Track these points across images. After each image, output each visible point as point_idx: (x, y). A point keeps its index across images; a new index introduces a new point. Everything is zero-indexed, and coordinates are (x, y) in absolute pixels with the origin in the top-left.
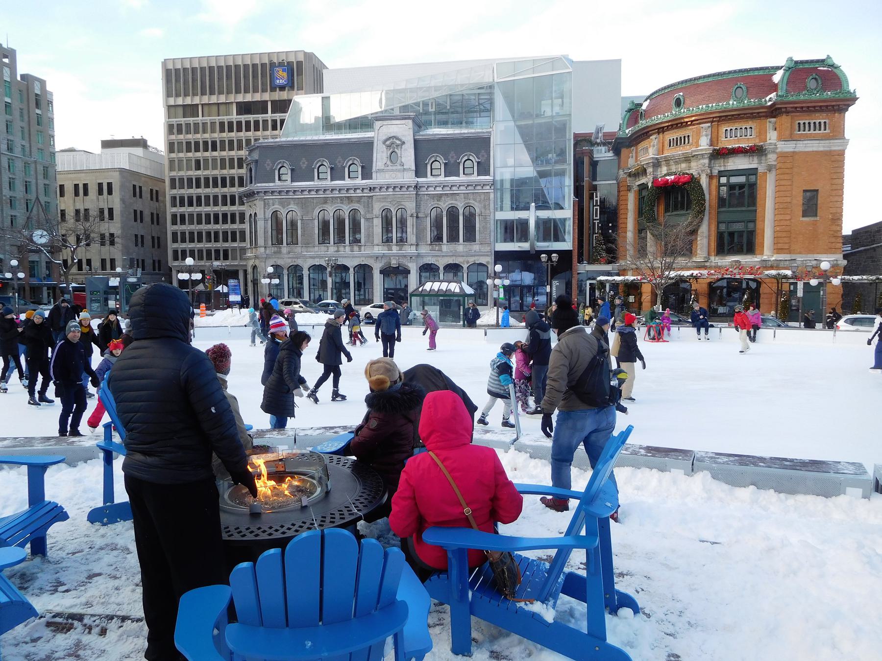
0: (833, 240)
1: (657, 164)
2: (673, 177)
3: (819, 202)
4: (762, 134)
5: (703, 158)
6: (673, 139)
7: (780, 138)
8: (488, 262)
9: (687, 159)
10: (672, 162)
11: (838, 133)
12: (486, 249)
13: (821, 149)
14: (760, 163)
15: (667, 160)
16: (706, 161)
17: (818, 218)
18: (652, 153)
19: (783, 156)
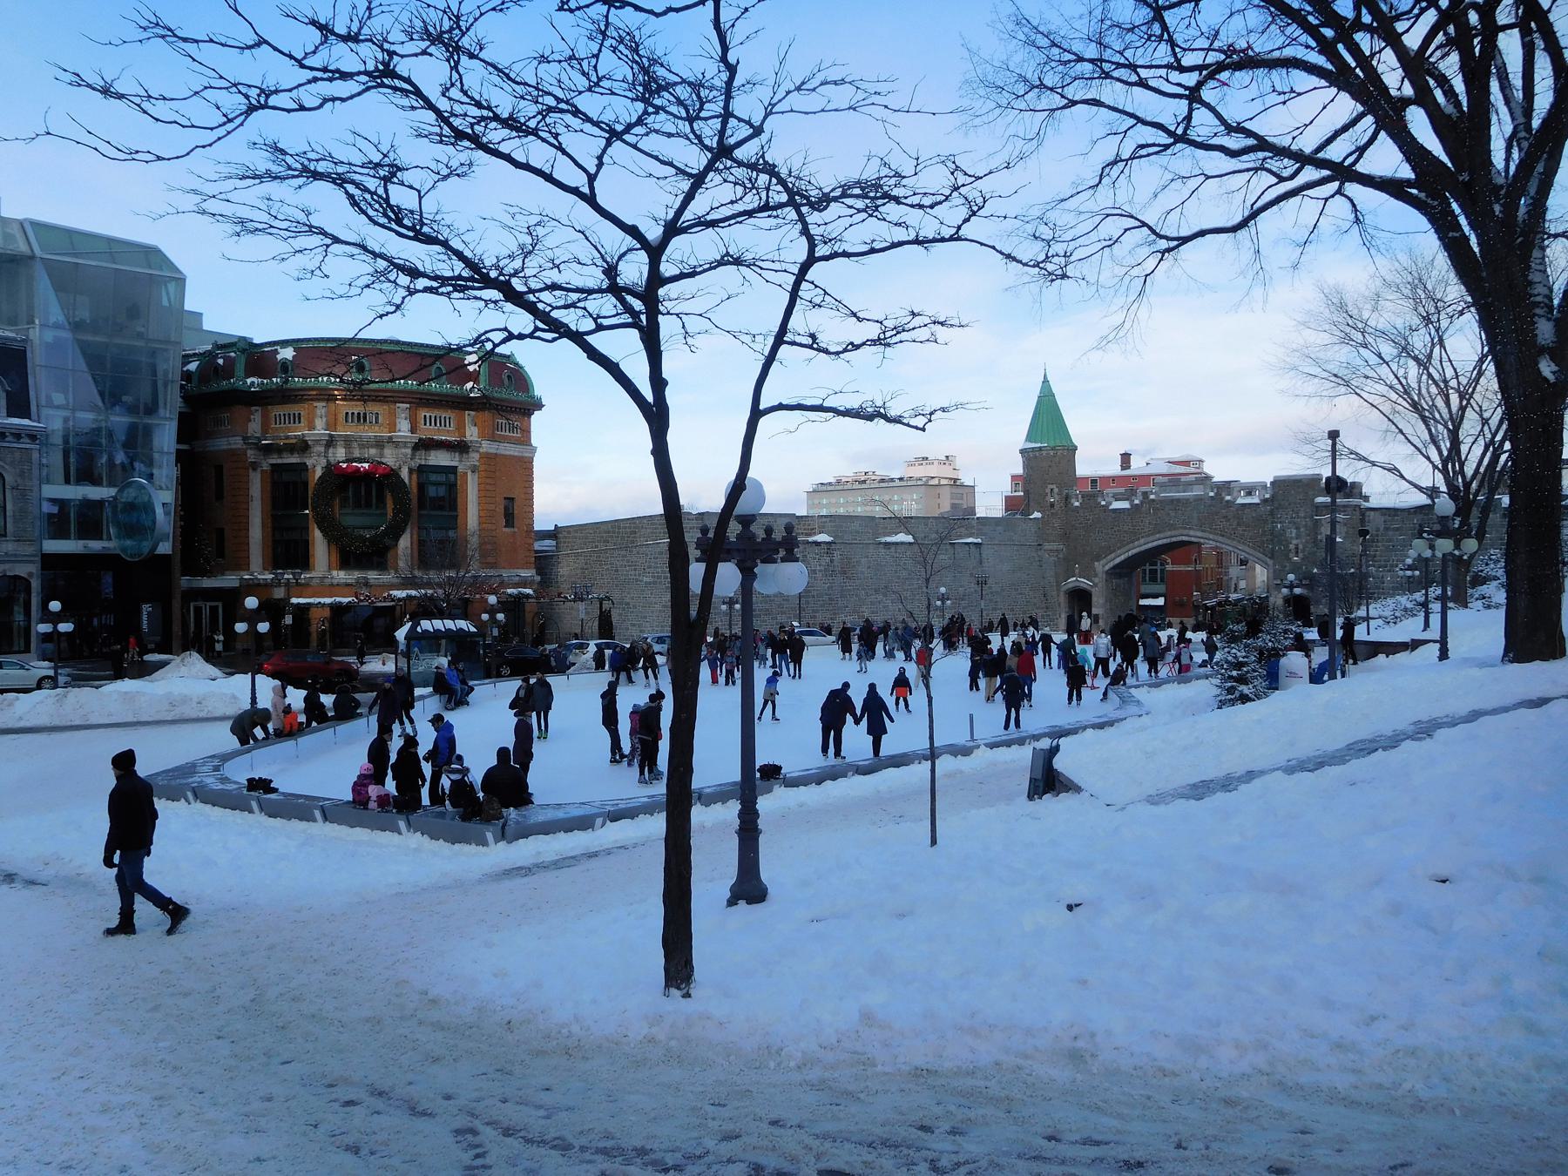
0: (528, 554)
1: (330, 442)
2: (366, 465)
3: (516, 512)
4: (461, 428)
5: (405, 447)
6: (353, 414)
7: (482, 435)
8: (31, 574)
9: (379, 444)
10: (355, 445)
11: (525, 438)
12: (28, 549)
13: (516, 454)
14: (461, 461)
15: (348, 442)
16: (409, 451)
17: (516, 530)
18: (320, 429)
19: (489, 458)
